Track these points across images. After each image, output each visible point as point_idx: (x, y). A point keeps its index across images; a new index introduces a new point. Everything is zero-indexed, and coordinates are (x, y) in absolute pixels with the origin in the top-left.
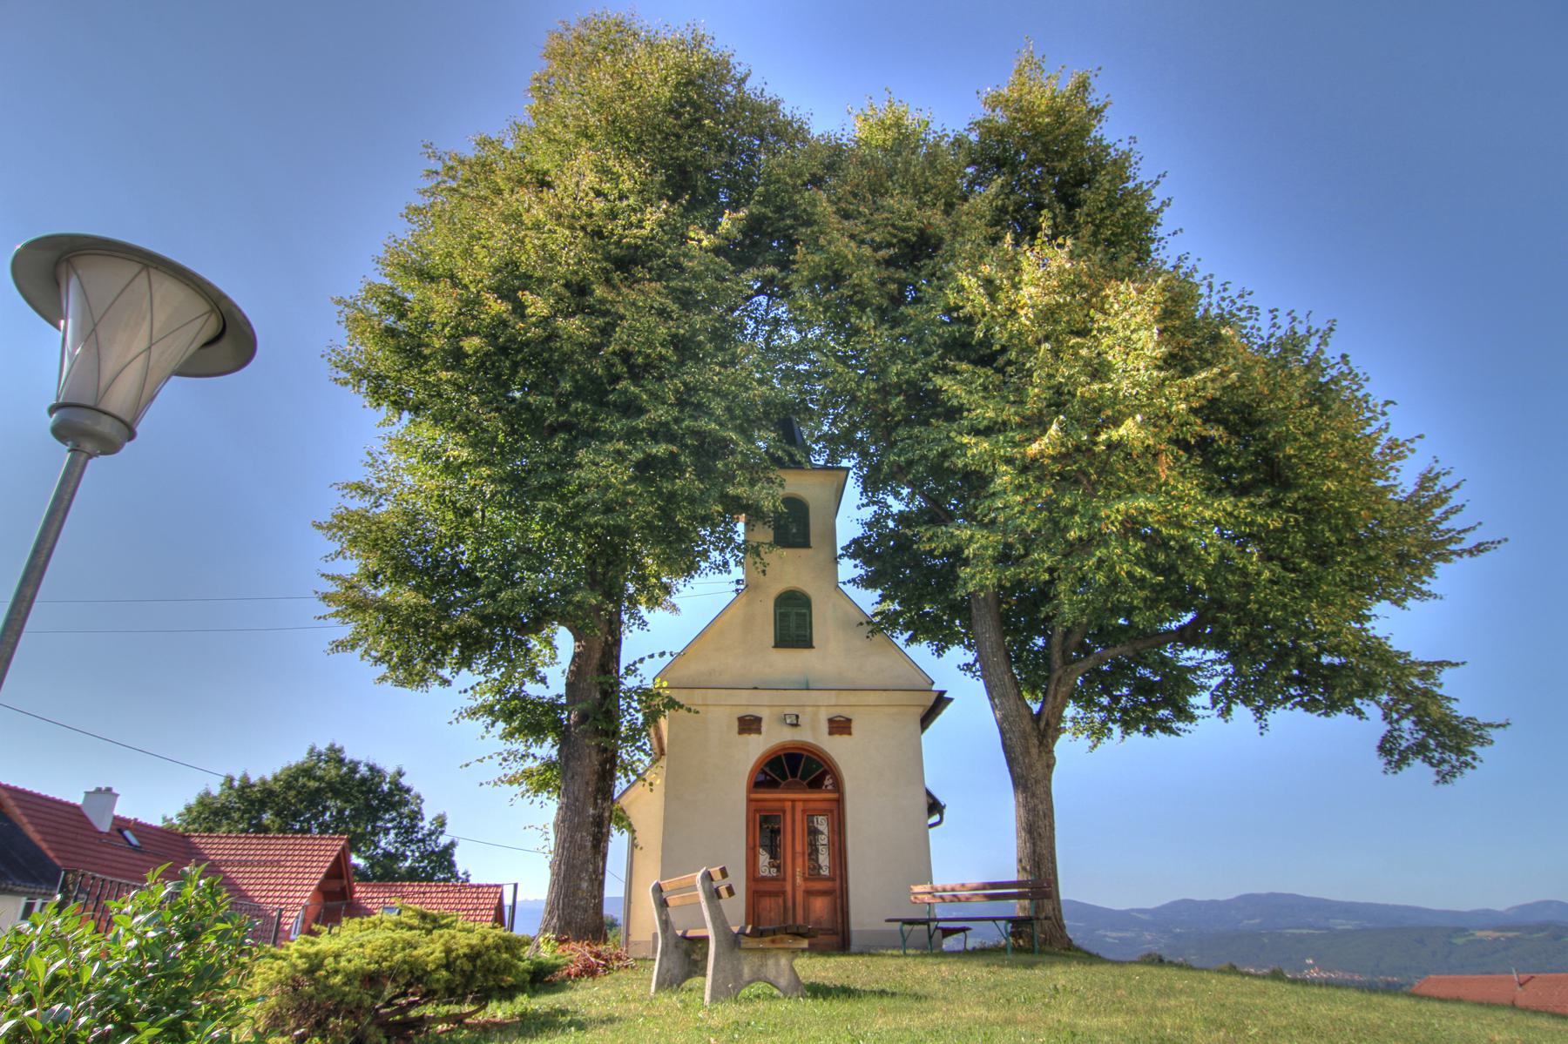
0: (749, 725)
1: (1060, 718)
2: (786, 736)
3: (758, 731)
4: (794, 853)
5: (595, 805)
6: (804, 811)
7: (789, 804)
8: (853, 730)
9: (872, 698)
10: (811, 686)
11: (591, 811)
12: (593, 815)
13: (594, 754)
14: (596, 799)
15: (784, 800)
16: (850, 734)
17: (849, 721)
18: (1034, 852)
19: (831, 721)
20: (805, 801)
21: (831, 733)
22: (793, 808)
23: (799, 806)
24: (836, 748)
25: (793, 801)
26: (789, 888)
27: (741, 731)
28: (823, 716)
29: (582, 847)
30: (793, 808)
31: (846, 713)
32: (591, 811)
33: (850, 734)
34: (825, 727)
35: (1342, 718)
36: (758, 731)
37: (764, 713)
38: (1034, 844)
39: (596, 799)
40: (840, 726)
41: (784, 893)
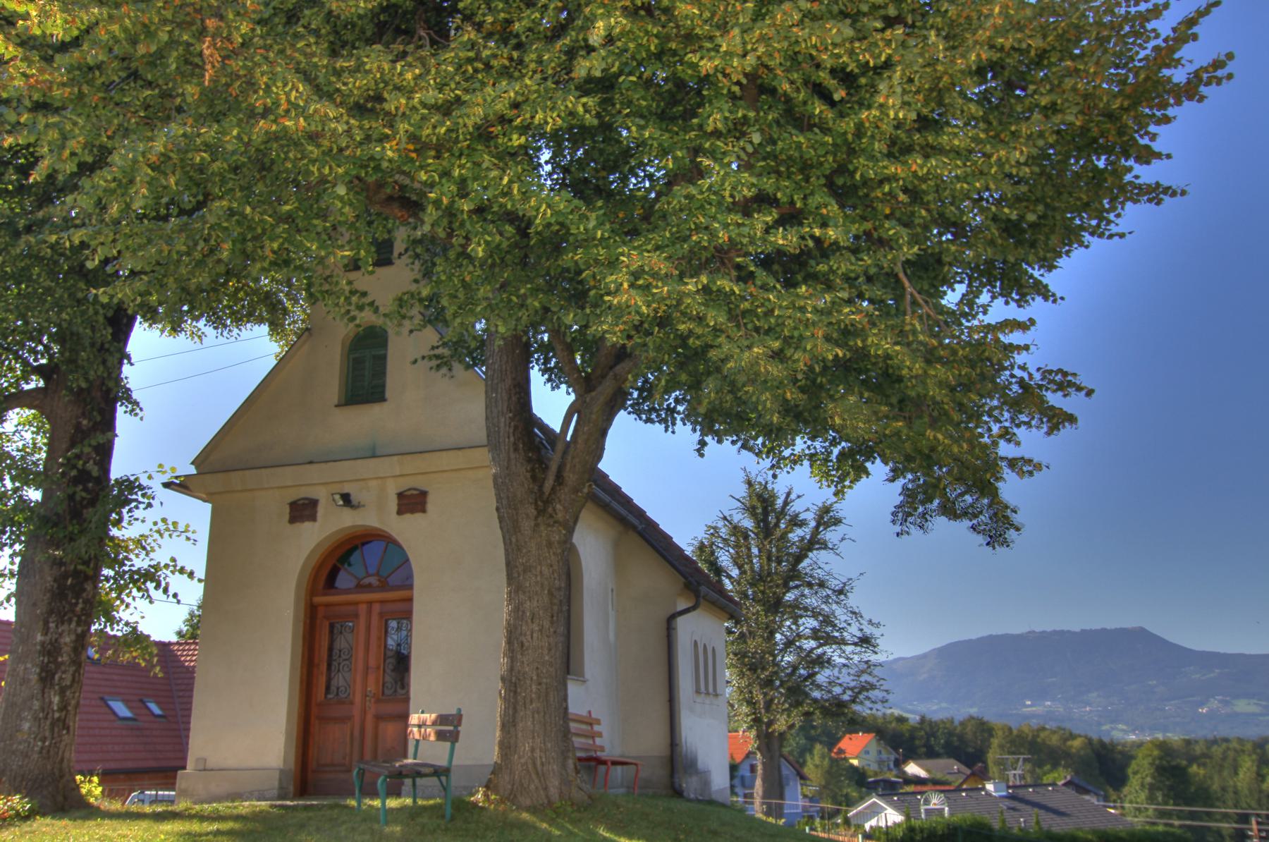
0: (303, 510)
1: (48, 452)
2: (348, 520)
3: (313, 518)
4: (367, 668)
5: (46, 631)
6: (381, 615)
7: (363, 609)
8: (429, 507)
9: (445, 460)
10: (378, 453)
11: (39, 638)
12: (43, 644)
13: (46, 568)
14: (46, 623)
15: (357, 603)
16: (424, 511)
17: (424, 494)
18: (511, 669)
19: (401, 496)
20: (382, 602)
21: (400, 512)
22: (370, 612)
23: (377, 608)
24: (405, 529)
25: (370, 603)
26: (356, 712)
27: (294, 519)
28: (392, 490)
29: (25, 681)
30: (370, 612)
31: (419, 483)
32: (39, 638)
33: (424, 511)
34: (393, 504)
35: (182, 341)
36: (313, 518)
37: (321, 494)
38: (512, 659)
39: (46, 623)
40: (413, 502)
41: (349, 718)
